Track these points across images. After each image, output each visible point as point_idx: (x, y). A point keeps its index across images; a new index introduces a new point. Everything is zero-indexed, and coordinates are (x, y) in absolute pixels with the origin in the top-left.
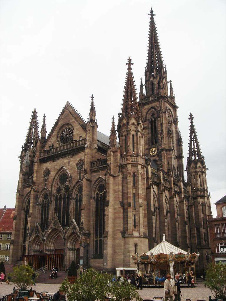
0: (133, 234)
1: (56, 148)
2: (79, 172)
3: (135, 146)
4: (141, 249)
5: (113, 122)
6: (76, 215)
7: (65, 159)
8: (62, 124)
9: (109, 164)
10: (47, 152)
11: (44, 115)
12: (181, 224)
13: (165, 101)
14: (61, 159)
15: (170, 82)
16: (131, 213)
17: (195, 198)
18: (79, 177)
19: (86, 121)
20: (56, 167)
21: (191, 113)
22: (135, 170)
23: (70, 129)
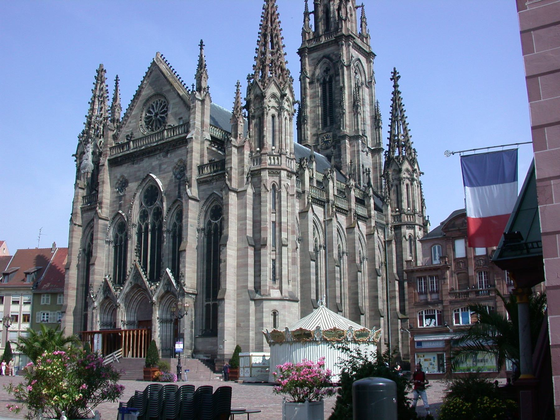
0: (269, 294)
1: (138, 139)
2: (177, 184)
3: (277, 137)
4: (285, 321)
5: (237, 93)
6: (174, 260)
7: (153, 160)
8: (149, 94)
9: (229, 169)
10: (121, 146)
11: (117, 77)
12: (369, 275)
13: (349, 45)
14: (146, 160)
15: (362, 6)
16: (268, 256)
17: (397, 228)
18: (177, 192)
19: (189, 90)
20: (138, 174)
21: (395, 69)
22: (276, 179)
23: (163, 104)
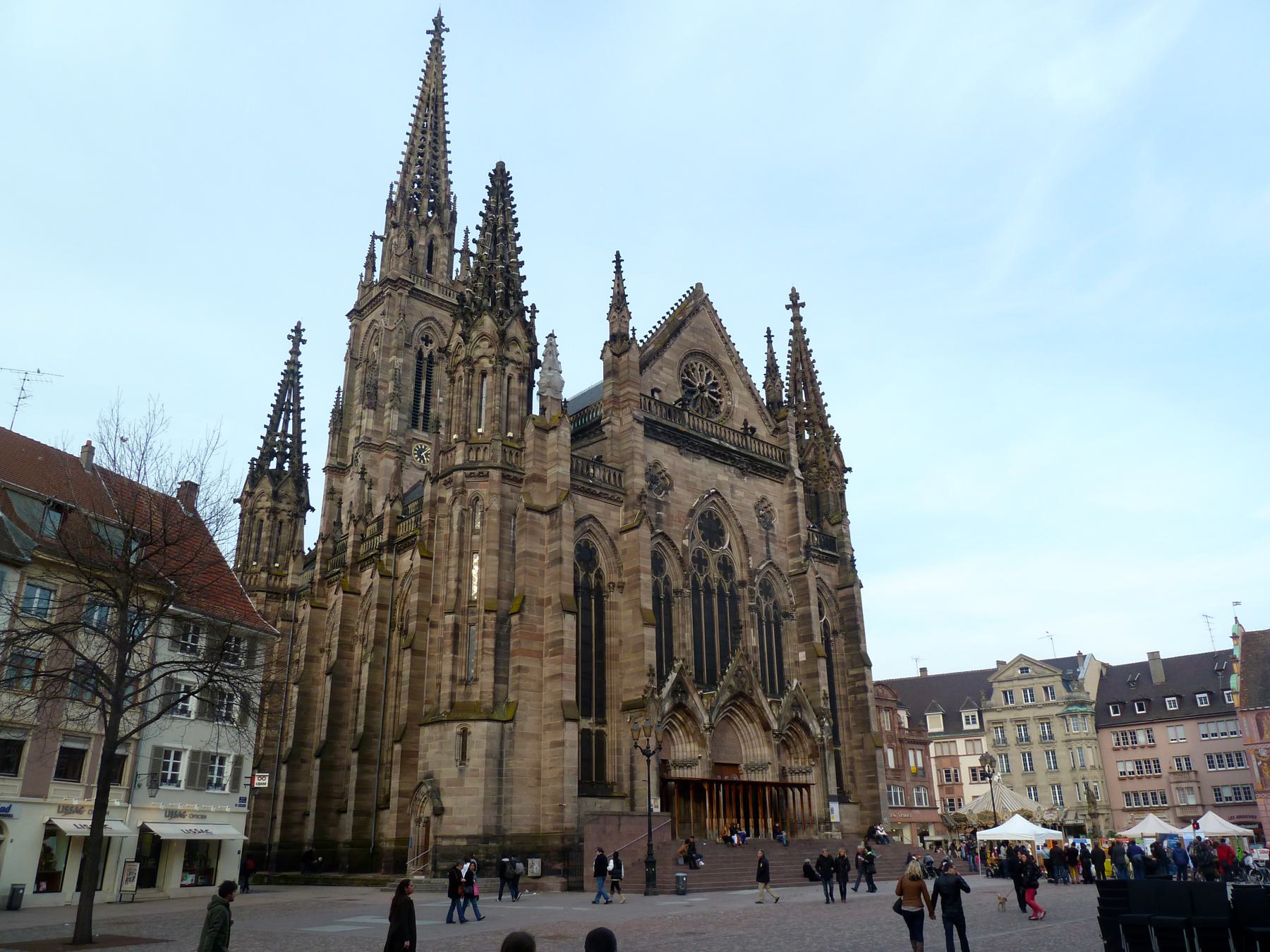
8: (693, 344)
11: (618, 255)
